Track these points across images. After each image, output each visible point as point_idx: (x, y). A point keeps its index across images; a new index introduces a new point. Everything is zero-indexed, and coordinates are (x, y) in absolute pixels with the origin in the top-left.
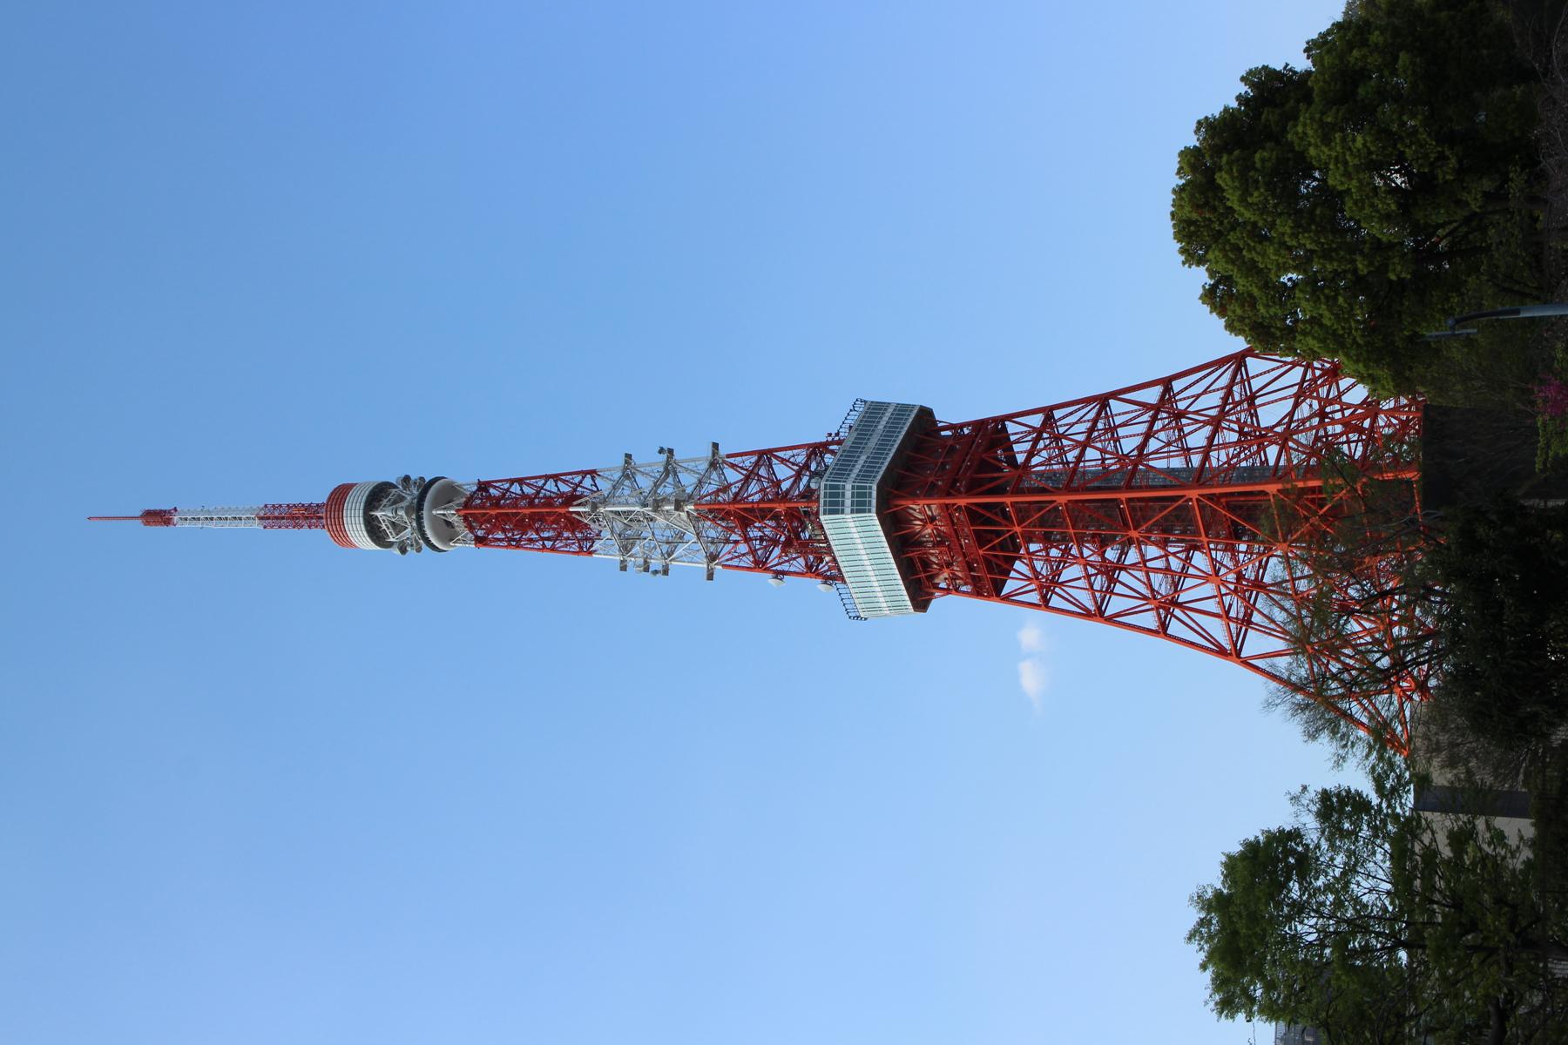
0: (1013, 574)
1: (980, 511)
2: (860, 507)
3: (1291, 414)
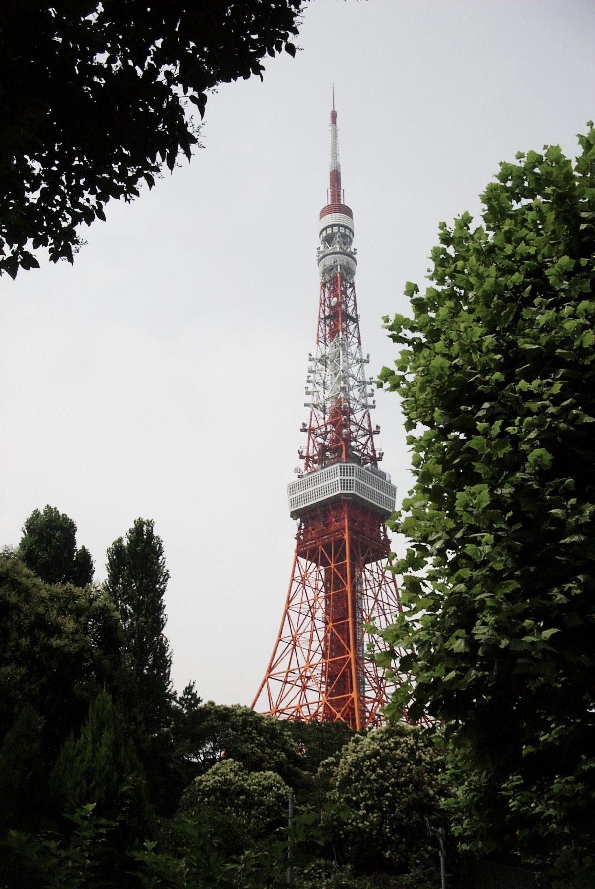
0: (309, 562)
1: (342, 545)
2: (344, 484)
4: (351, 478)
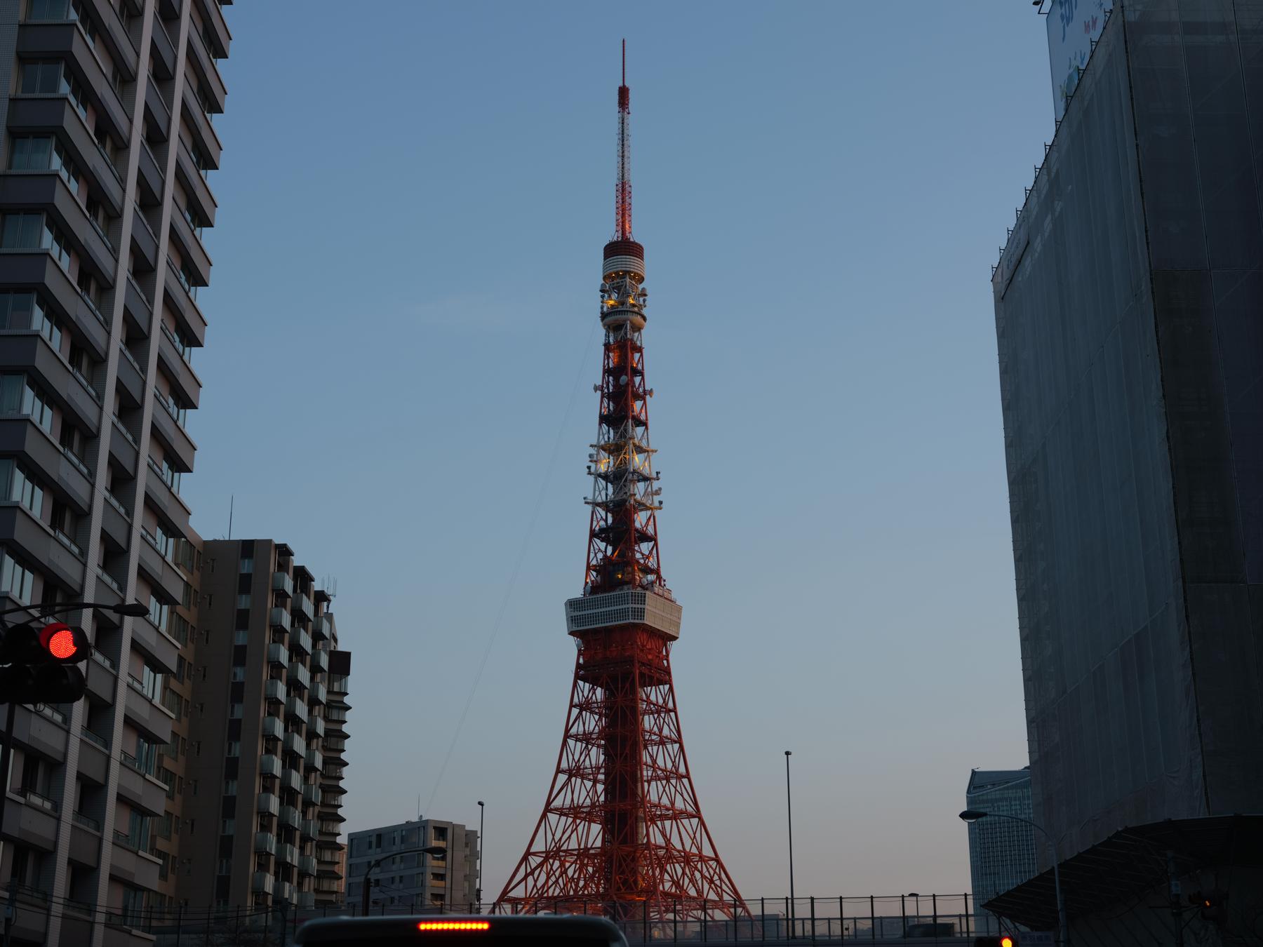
3: (675, 849)
4: (642, 606)
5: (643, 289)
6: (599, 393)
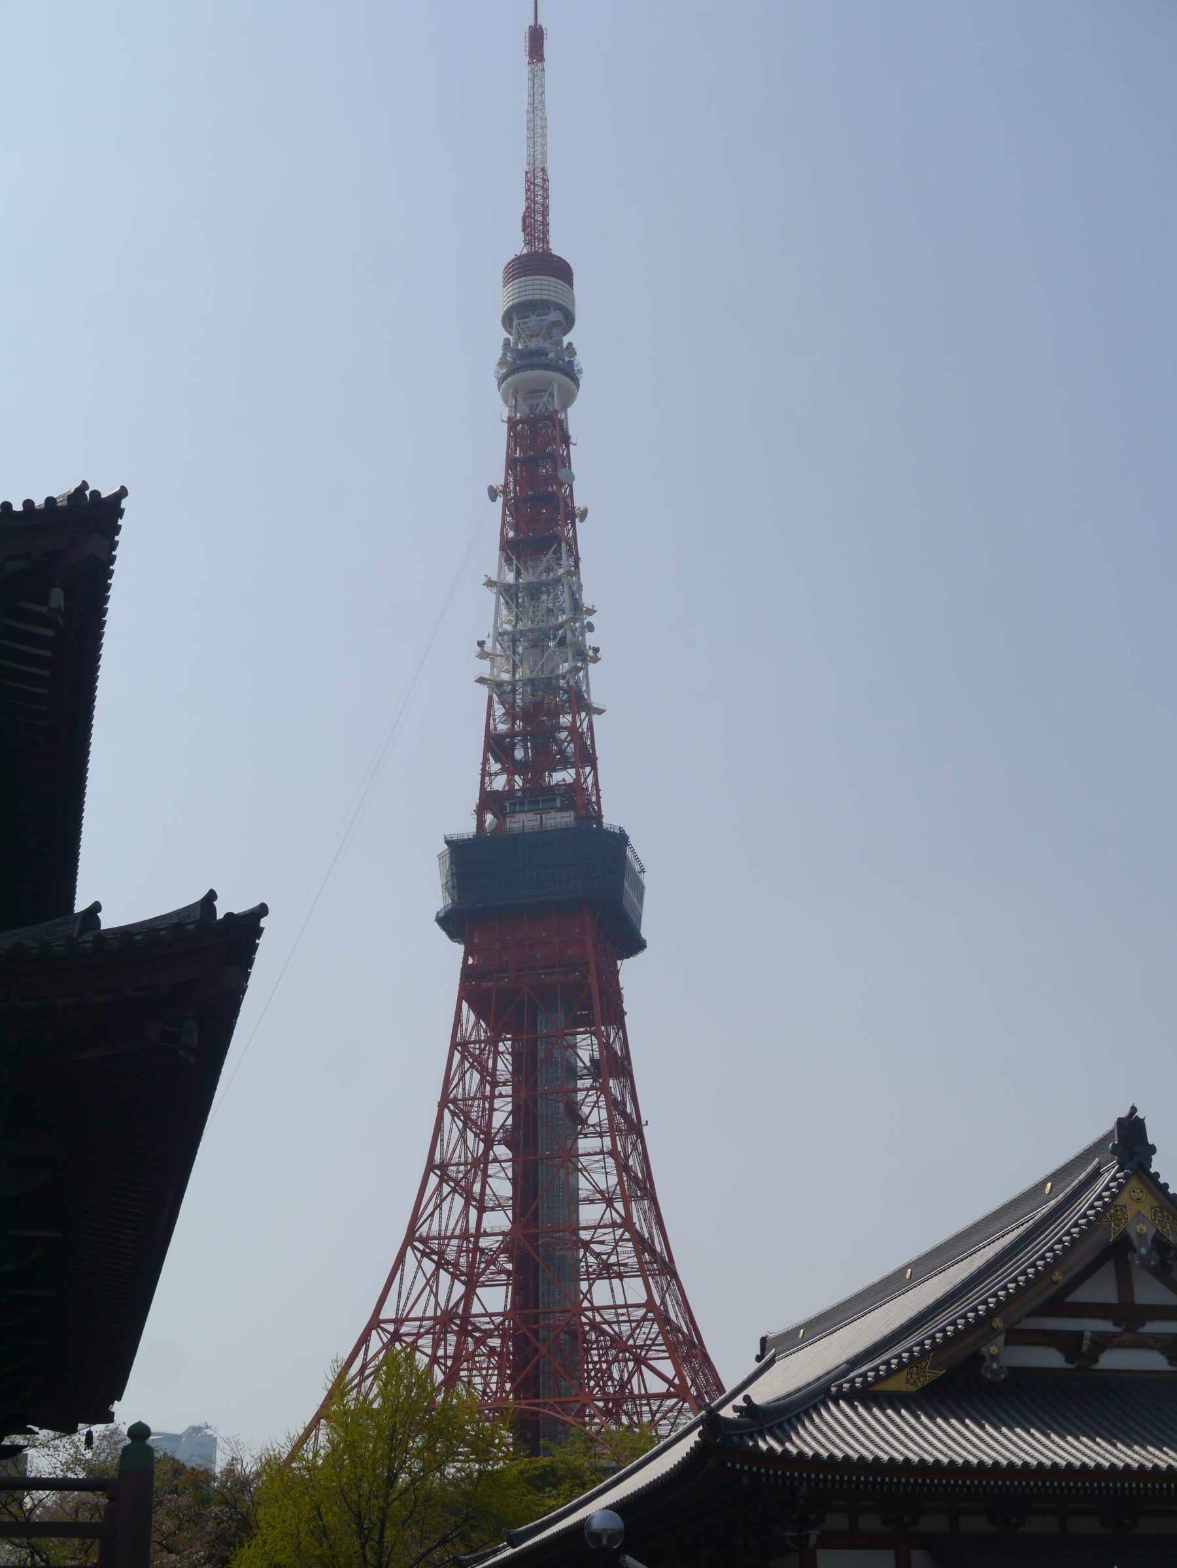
5: (570, 344)
6: (500, 500)
